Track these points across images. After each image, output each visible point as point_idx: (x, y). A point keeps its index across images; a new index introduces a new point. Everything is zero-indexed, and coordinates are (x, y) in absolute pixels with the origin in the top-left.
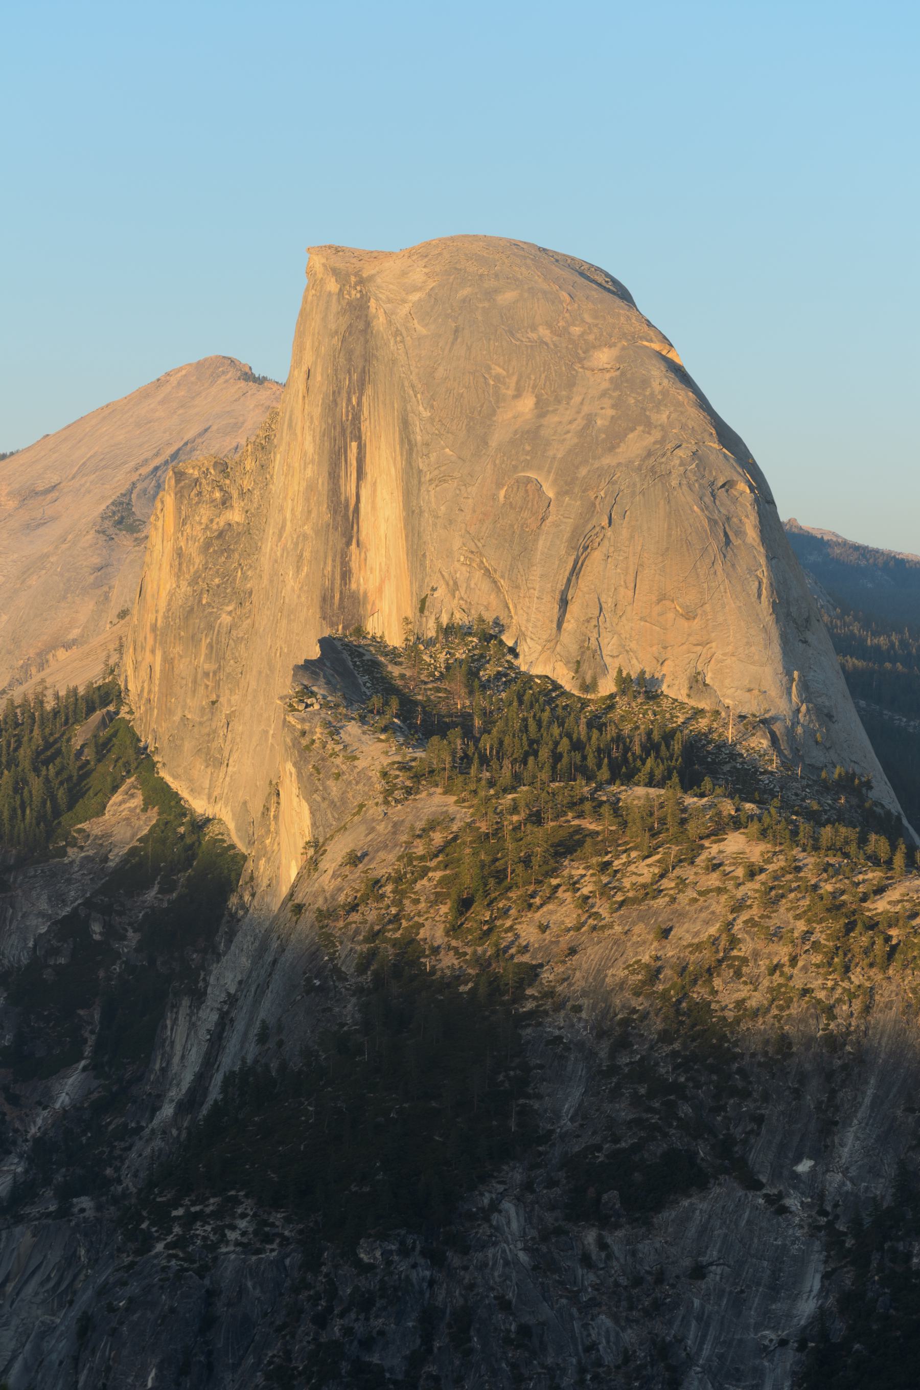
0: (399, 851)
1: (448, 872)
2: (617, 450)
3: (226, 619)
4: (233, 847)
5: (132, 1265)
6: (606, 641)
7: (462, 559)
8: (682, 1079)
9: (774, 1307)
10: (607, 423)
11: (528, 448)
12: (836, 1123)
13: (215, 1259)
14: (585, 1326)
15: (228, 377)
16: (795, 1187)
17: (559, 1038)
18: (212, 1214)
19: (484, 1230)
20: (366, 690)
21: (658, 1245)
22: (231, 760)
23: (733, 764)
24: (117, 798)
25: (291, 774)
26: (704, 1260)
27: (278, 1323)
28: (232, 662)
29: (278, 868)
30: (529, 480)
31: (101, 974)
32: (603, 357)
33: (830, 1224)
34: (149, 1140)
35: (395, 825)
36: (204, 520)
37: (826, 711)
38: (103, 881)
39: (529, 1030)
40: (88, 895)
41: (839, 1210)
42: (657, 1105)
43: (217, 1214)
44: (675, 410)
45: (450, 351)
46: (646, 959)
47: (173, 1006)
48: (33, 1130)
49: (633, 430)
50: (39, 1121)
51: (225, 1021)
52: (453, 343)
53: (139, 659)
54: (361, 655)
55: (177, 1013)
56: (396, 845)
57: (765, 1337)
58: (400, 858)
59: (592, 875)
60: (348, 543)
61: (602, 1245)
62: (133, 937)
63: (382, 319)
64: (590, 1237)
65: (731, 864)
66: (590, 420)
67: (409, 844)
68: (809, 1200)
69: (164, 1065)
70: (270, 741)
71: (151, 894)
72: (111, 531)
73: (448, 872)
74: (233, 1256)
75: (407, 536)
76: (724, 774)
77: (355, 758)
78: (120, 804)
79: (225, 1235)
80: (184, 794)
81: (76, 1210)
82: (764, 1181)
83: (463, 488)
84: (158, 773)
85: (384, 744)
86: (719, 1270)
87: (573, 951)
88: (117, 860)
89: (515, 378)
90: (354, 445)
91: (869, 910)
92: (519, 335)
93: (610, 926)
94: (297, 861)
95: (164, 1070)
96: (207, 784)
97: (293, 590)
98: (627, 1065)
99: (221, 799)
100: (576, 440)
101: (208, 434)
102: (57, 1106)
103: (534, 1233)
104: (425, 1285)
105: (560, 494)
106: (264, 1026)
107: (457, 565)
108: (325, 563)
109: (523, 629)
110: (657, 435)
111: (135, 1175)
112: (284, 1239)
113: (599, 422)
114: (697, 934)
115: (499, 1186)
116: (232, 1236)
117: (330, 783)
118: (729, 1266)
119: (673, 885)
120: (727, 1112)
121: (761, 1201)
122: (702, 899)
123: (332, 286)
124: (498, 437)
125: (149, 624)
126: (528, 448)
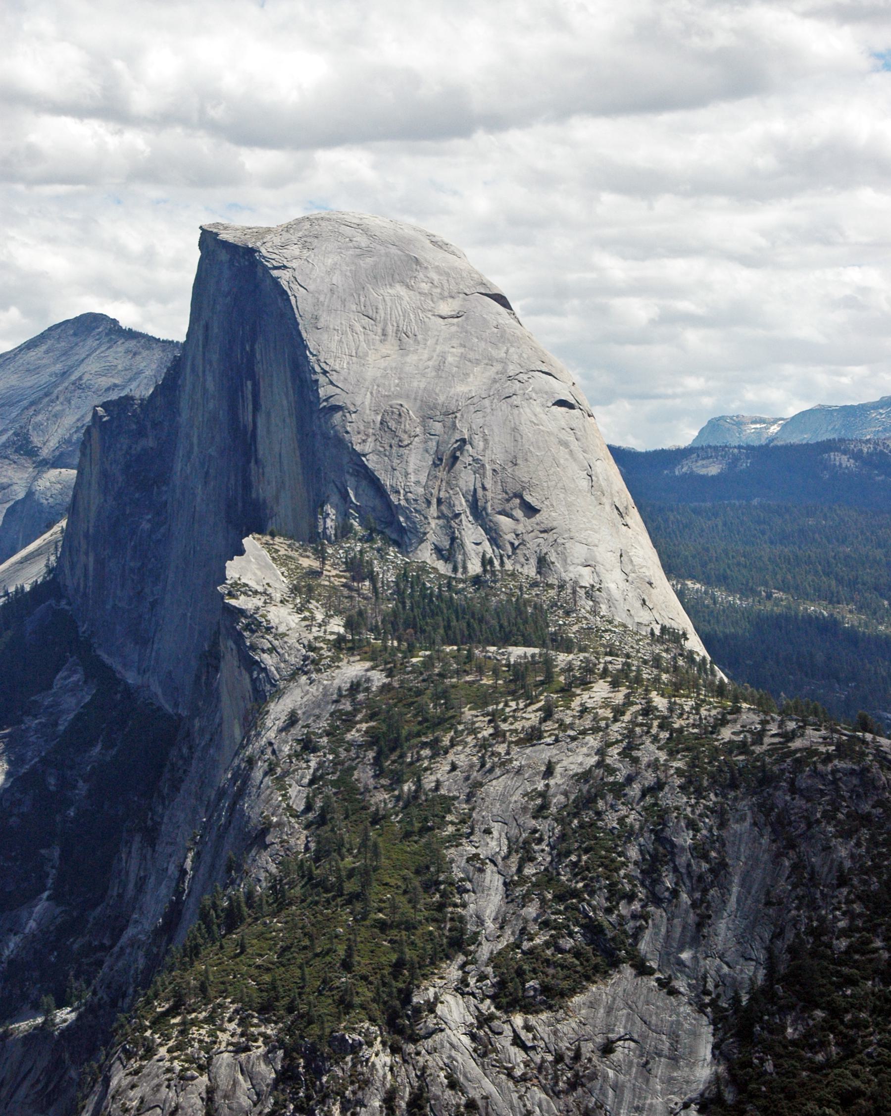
0: (332, 708)
1: (372, 724)
2: (469, 380)
3: (146, 526)
4: (160, 708)
5: (141, 1067)
6: (470, 532)
7: (351, 470)
8: (580, 885)
9: (675, 1074)
10: (457, 359)
11: (397, 381)
12: (709, 917)
13: (210, 1059)
14: (520, 1098)
15: (100, 330)
16: (681, 972)
17: (476, 856)
18: (207, 1021)
19: (431, 1022)
20: (284, 579)
21: (574, 1025)
22: (156, 638)
23: (580, 625)
24: (61, 675)
25: (232, 649)
26: (612, 1036)
27: (267, 1110)
28: (153, 559)
29: (220, 725)
30: (401, 405)
31: (58, 818)
33: (713, 1003)
34: (118, 958)
35: (325, 687)
36: (125, 447)
37: (647, 580)
38: (55, 742)
39: (452, 850)
40: (43, 754)
41: (720, 989)
42: (562, 908)
43: (210, 1020)
44: (512, 346)
45: (328, 306)
46: (540, 786)
47: (126, 843)
48: (7, 952)
49: (477, 362)
50: (12, 945)
52: (330, 300)
53: (75, 559)
54: (277, 551)
55: (130, 848)
56: (328, 703)
57: (671, 1100)
58: (332, 715)
59: (490, 722)
60: (249, 462)
61: (528, 1028)
62: (83, 788)
63: (268, 281)
65: (601, 708)
66: (443, 357)
67: (336, 702)
68: (694, 982)
69: (121, 891)
70: (189, 621)
71: (97, 750)
72: (15, 457)
73: (372, 724)
74: (226, 1055)
75: (301, 455)
76: (574, 633)
77: (286, 635)
78: (65, 678)
79: (217, 1037)
80: (119, 668)
81: (58, 1020)
82: (655, 966)
83: (348, 415)
84: (95, 651)
85: (307, 623)
86: (627, 1044)
87: (481, 785)
88: (66, 724)
89: (381, 326)
90: (249, 383)
91: (717, 740)
92: (382, 292)
93: (511, 761)
94: (239, 720)
95: (120, 896)
96: (136, 657)
97: (202, 500)
98: (533, 875)
99: (149, 670)
100: (434, 374)
101: (85, 378)
102: (27, 931)
103: (471, 1020)
104: (387, 1069)
105: (426, 419)
107: (348, 477)
108: (229, 478)
109: (404, 524)
110: (498, 367)
111: (109, 987)
112: (266, 1037)
113: (450, 359)
114: (581, 764)
115: (439, 981)
116: (224, 1037)
117: (265, 656)
118: (634, 1041)
119: (557, 725)
120: (619, 911)
122: (580, 736)
123: (224, 256)
124: (370, 373)
125: (81, 533)
126: (397, 381)
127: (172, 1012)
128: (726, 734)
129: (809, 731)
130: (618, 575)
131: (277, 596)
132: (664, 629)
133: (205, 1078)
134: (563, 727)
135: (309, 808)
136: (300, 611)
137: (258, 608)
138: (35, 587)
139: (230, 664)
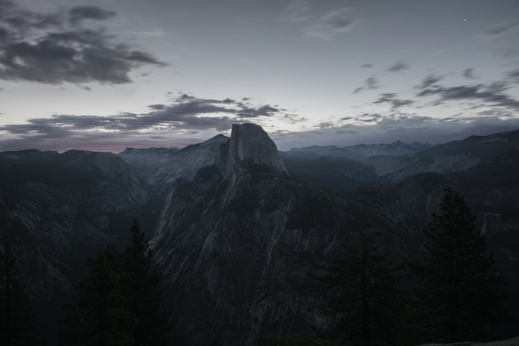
3: (225, 158)
17: (261, 197)
32: (260, 134)
46: (269, 189)
51: (229, 195)
63: (240, 131)
64: (265, 215)
71: (219, 183)
80: (222, 174)
82: (281, 209)
106: (234, 196)
116: (232, 215)
121: (281, 211)
123: (235, 128)
127: (227, 213)
128: (290, 184)
129: (299, 183)
130: (279, 165)
131: (240, 167)
132: (284, 171)
133: (230, 220)
134: (272, 182)
135: (242, 190)
136: (242, 168)
137: (237, 168)
138: (213, 165)
139: (234, 174)
